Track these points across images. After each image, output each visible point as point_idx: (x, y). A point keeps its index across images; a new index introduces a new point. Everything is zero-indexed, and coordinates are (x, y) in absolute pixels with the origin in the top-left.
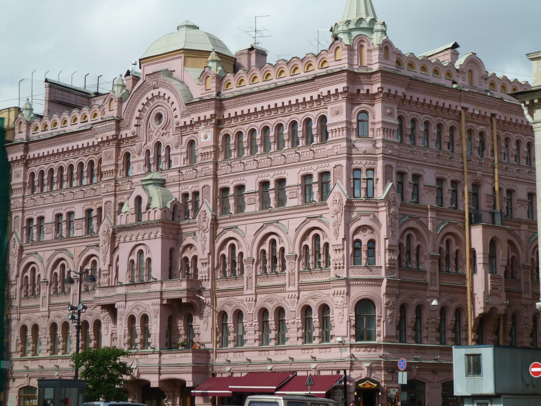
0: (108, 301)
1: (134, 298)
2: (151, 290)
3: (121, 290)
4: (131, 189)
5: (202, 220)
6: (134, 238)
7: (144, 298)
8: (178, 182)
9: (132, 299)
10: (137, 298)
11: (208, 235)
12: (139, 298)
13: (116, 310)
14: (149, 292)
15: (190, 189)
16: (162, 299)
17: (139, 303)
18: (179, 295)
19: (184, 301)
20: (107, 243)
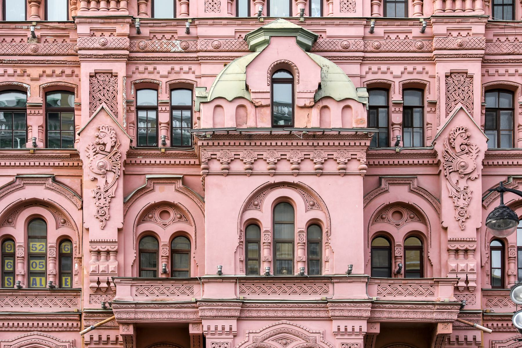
0: (166, 316)
1: (271, 314)
2: (328, 296)
3: (212, 291)
4: (186, 50)
5: (458, 149)
6: (261, 167)
7: (305, 314)
8: (362, 54)
9: (263, 314)
10: (280, 314)
11: (477, 188)
12: (288, 314)
13: (202, 339)
14: (326, 302)
15: (396, 74)
16: (370, 321)
17: (284, 325)
18: (429, 316)
19: (441, 330)
20: (111, 177)
